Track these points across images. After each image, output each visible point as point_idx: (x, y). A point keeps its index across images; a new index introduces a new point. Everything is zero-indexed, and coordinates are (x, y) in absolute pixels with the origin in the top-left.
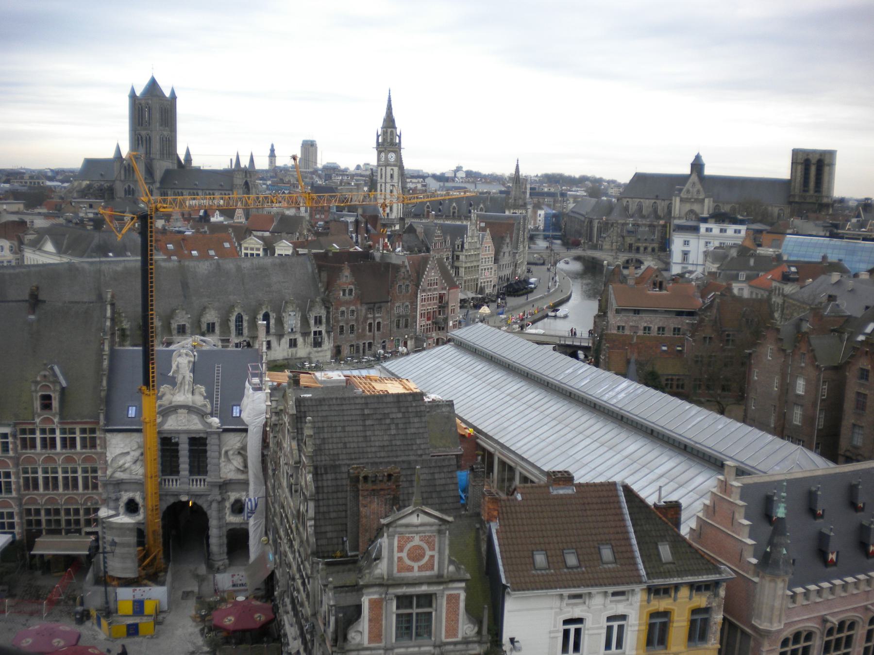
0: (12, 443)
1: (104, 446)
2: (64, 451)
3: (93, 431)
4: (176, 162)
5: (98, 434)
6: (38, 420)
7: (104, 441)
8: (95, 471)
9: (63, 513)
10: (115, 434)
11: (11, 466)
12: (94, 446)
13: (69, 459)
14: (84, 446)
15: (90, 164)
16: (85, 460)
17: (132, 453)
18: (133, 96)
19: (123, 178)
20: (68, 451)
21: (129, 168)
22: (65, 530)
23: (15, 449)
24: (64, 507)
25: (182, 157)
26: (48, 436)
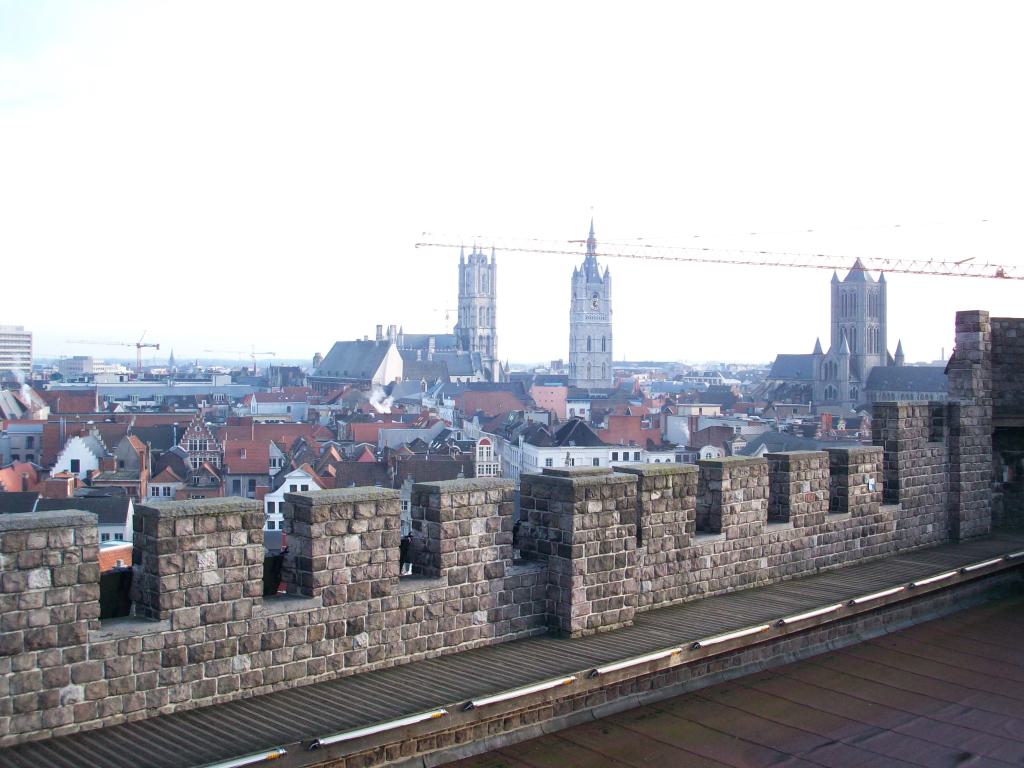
4: (886, 358)
15: (785, 364)
18: (835, 280)
19: (823, 378)
21: (831, 369)
25: (893, 353)
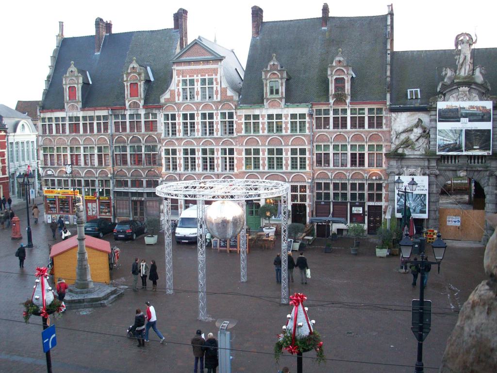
0: (308, 122)
1: (389, 125)
2: (354, 130)
3: (380, 110)
5: (384, 114)
6: (332, 101)
7: (389, 120)
8: (380, 147)
9: (349, 187)
10: (400, 114)
11: (307, 143)
12: (380, 125)
13: (357, 137)
14: (371, 125)
16: (371, 138)
17: (415, 130)
20: (357, 130)
22: (350, 203)
23: (311, 129)
24: (351, 182)
26: (340, 116)
